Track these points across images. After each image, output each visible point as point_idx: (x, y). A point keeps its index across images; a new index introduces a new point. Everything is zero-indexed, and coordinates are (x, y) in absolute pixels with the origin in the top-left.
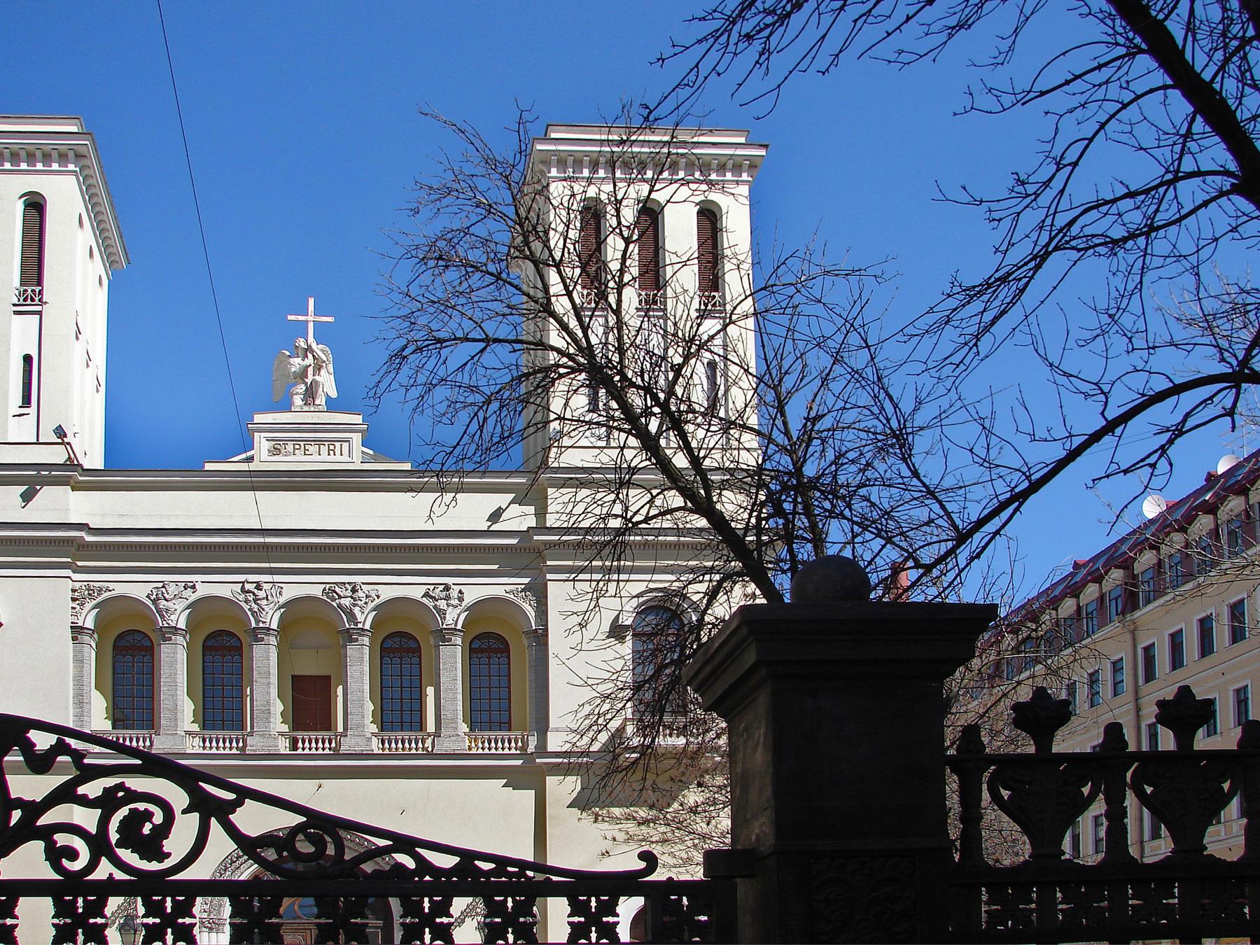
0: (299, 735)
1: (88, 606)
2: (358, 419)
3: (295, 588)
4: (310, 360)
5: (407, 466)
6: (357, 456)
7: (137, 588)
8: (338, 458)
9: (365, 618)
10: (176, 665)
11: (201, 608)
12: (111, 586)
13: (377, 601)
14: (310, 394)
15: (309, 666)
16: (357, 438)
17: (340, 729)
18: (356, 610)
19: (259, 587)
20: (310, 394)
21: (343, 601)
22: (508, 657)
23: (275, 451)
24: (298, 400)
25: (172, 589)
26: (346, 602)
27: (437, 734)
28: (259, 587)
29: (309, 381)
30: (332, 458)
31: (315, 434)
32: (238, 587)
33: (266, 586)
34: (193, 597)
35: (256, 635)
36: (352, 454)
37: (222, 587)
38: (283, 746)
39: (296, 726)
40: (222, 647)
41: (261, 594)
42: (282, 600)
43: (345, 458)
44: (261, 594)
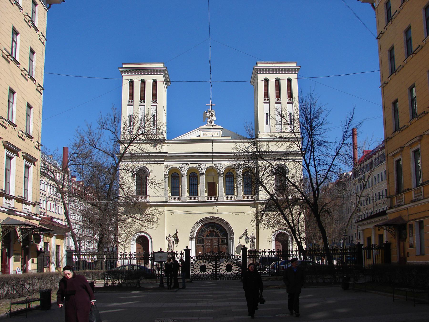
0: (209, 196)
1: (167, 169)
2: (221, 127)
3: (209, 164)
4: (211, 114)
5: (230, 138)
6: (221, 135)
7: (177, 165)
8: (217, 136)
9: (222, 171)
10: (184, 181)
11: (190, 169)
14: (211, 121)
15: (211, 180)
16: (221, 132)
17: (217, 195)
18: (221, 169)
19: (201, 164)
20: (211, 121)
23: (204, 134)
24: (209, 123)
25: (184, 165)
26: (219, 167)
27: (237, 196)
28: (201, 164)
29: (211, 118)
30: (217, 136)
31: (212, 131)
34: (188, 167)
35: (201, 175)
36: (219, 135)
37: (193, 164)
38: (206, 198)
39: (208, 195)
40: (194, 176)
41: (202, 166)
42: (206, 167)
43: (218, 136)
44: (202, 166)
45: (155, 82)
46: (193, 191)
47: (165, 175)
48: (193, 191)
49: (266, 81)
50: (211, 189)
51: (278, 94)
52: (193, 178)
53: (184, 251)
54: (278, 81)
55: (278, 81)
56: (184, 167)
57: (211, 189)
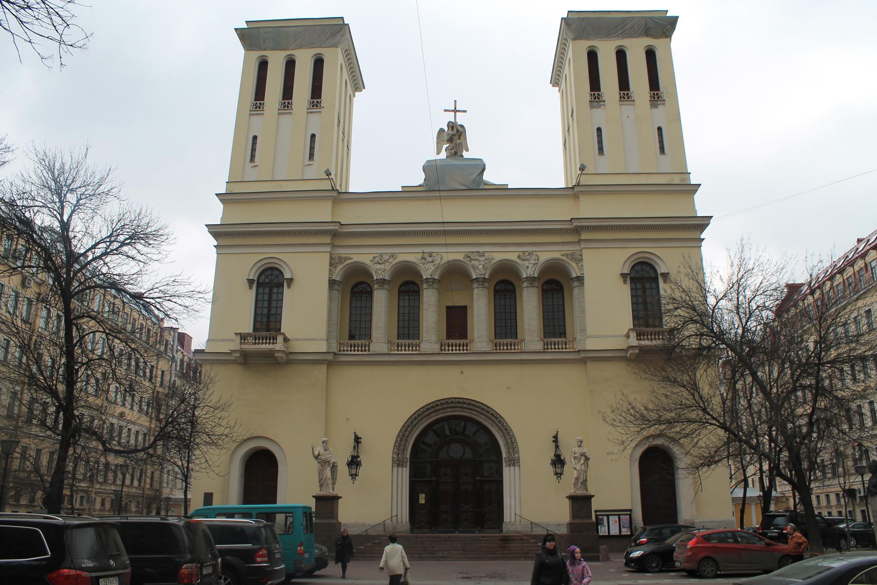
12: (351, 256)
13: (493, 262)
21: (473, 262)
22: (563, 294)
26: (476, 263)
32: (419, 256)
33: (434, 255)
34: (395, 262)
41: (430, 259)
45: (319, 64)
46: (408, 328)
47: (332, 283)
48: (408, 328)
49: (592, 56)
50: (456, 323)
51: (624, 83)
52: (407, 297)
54: (621, 55)
55: (621, 55)
57: (456, 323)
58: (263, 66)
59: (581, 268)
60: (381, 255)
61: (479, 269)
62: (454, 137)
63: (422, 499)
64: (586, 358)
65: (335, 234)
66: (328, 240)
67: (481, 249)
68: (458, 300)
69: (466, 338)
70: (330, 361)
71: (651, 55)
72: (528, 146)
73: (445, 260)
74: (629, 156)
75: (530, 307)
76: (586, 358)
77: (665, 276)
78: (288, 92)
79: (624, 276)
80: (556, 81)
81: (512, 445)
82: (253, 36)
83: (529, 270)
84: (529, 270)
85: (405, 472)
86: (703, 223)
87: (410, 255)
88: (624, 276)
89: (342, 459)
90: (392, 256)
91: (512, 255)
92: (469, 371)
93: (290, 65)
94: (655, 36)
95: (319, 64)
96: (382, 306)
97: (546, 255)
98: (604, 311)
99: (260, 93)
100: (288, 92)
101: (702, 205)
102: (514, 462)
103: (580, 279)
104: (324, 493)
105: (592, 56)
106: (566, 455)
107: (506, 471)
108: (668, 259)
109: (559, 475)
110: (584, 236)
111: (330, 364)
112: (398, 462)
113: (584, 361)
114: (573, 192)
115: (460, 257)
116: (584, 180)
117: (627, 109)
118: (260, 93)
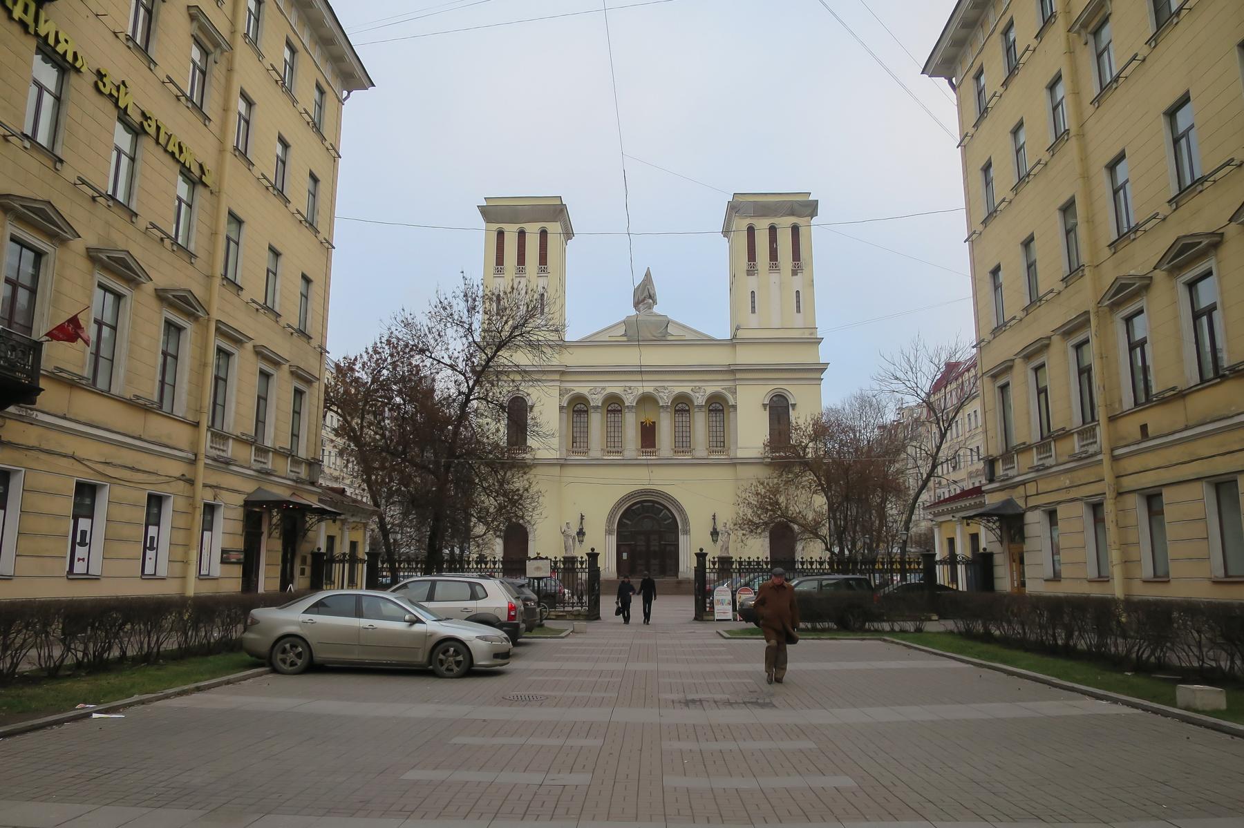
7: (582, 389)
45: (544, 234)
46: (614, 443)
47: (561, 408)
49: (751, 230)
50: (648, 435)
51: (773, 255)
53: (586, 557)
54: (773, 230)
56: (594, 391)
57: (648, 435)
58: (501, 234)
59: (735, 399)
60: (595, 388)
61: (665, 399)
62: (644, 296)
63: (625, 556)
64: (734, 463)
65: (563, 373)
66: (557, 377)
67: (666, 384)
68: (649, 417)
69: (654, 446)
70: (562, 464)
71: (795, 230)
72: (703, 296)
73: (641, 392)
74: (774, 314)
75: (700, 423)
76: (734, 463)
77: (794, 406)
78: (521, 259)
79: (765, 405)
80: (726, 232)
81: (686, 521)
82: (490, 212)
83: (700, 399)
84: (700, 399)
85: (614, 538)
86: (821, 368)
87: (615, 388)
88: (765, 405)
89: (574, 533)
90: (604, 388)
91: (686, 388)
92: (657, 470)
93: (522, 234)
94: (799, 216)
95: (544, 234)
96: (596, 421)
97: (711, 389)
98: (751, 431)
99: (500, 260)
100: (521, 259)
101: (824, 354)
102: (687, 532)
103: (735, 407)
104: (568, 555)
105: (751, 230)
106: (720, 528)
107: (681, 538)
108: (796, 393)
109: (715, 541)
110: (738, 376)
111: (562, 465)
112: (609, 532)
113: (735, 464)
114: (733, 342)
115: (651, 390)
116: (741, 334)
117: (774, 277)
118: (500, 260)
